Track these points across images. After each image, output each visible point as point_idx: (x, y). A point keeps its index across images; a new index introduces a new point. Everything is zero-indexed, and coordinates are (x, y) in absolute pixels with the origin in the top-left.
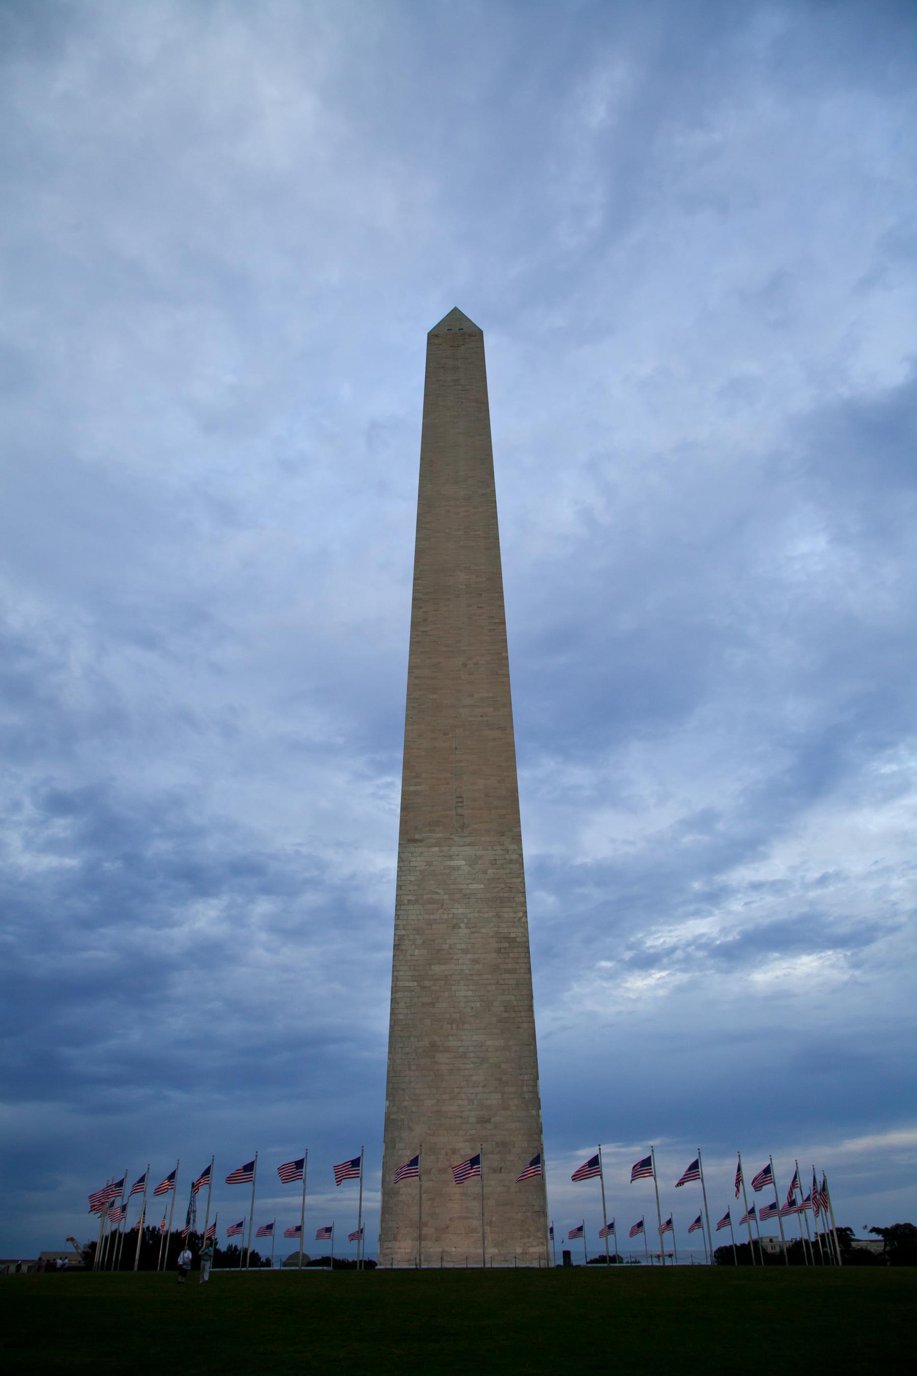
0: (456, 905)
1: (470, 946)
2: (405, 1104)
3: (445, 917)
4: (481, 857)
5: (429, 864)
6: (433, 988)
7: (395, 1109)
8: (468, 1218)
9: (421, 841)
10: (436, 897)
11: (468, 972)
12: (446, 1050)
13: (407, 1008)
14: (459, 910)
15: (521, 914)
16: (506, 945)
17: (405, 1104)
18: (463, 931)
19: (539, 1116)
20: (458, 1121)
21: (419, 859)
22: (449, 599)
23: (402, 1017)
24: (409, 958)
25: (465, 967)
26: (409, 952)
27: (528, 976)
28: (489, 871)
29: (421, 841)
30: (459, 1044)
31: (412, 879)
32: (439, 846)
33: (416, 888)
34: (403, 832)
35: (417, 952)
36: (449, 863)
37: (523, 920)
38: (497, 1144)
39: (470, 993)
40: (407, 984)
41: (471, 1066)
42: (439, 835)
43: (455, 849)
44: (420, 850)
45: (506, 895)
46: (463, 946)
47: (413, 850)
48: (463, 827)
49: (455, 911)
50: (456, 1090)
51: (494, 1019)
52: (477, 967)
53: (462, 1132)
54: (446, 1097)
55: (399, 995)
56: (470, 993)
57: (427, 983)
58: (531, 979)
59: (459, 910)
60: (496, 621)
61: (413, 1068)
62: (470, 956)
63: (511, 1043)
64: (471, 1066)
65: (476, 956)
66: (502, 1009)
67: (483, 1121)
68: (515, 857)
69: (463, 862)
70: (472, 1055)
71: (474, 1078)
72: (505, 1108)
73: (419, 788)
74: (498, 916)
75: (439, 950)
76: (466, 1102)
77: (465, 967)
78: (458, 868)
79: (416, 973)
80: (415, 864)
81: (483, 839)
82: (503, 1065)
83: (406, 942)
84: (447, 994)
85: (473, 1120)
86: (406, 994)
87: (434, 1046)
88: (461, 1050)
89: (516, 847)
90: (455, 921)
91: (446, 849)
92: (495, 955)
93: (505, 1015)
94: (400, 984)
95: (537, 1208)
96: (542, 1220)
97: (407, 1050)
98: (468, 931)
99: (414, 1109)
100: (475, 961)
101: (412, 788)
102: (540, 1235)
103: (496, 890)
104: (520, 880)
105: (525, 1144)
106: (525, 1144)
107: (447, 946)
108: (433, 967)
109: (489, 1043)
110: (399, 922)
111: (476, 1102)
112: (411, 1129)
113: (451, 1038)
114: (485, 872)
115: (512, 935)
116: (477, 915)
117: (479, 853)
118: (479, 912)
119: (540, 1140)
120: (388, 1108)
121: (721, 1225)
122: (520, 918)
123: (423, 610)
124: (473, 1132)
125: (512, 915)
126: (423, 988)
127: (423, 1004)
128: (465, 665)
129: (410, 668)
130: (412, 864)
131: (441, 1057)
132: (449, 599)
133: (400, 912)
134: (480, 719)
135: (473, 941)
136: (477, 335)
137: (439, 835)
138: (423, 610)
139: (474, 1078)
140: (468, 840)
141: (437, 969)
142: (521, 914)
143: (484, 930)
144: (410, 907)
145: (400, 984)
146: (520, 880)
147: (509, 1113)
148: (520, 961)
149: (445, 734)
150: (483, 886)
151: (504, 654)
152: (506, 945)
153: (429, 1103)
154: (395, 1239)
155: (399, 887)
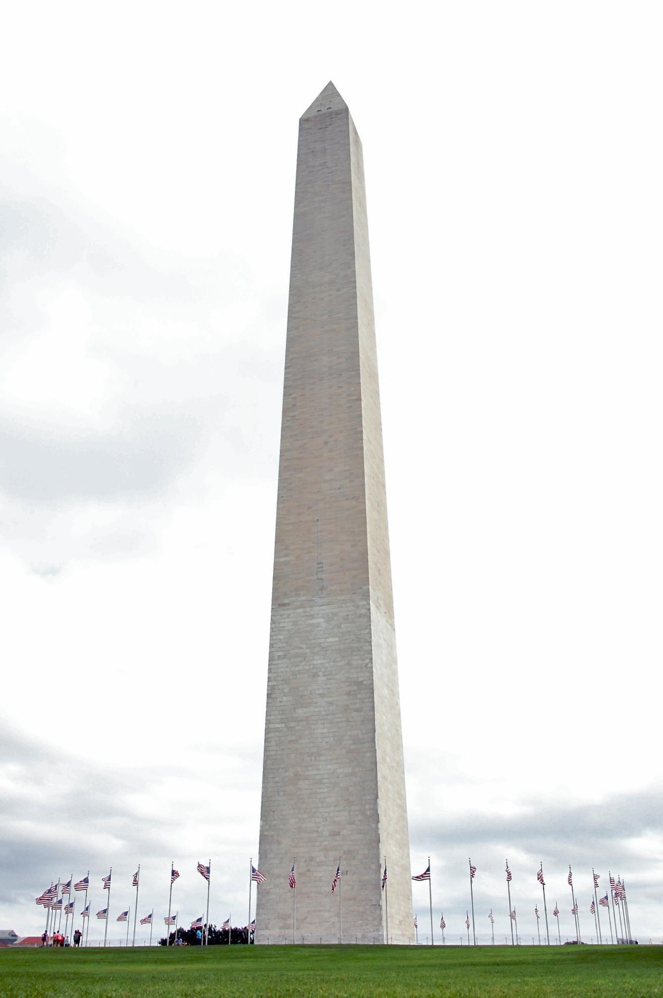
0: (316, 657)
1: (326, 691)
2: (274, 823)
3: (307, 667)
4: (336, 614)
5: (295, 623)
6: (297, 728)
7: (267, 827)
8: (320, 911)
9: (289, 604)
10: (301, 651)
11: (324, 713)
12: (307, 778)
13: (277, 745)
14: (318, 661)
16: (355, 688)
17: (274, 823)
18: (322, 679)
19: (377, 828)
20: (314, 835)
21: (287, 620)
22: (313, 384)
23: (273, 753)
24: (278, 704)
25: (322, 709)
26: (279, 700)
27: (371, 713)
28: (343, 626)
29: (289, 604)
30: (316, 772)
31: (281, 637)
32: (304, 607)
33: (285, 645)
34: (275, 599)
35: (285, 699)
36: (311, 622)
37: (369, 665)
38: (345, 852)
39: (325, 730)
40: (277, 726)
41: (326, 790)
43: (316, 609)
45: (356, 645)
46: (321, 691)
47: (282, 612)
48: (322, 589)
49: (315, 662)
50: (314, 810)
51: (344, 751)
52: (331, 708)
53: (317, 844)
54: (305, 816)
56: (325, 730)
57: (292, 724)
58: (374, 715)
59: (318, 661)
60: (354, 398)
61: (281, 794)
62: (326, 699)
63: (357, 769)
64: (326, 790)
65: (331, 699)
66: (351, 742)
67: (335, 834)
68: (363, 611)
69: (322, 620)
70: (326, 781)
71: (328, 800)
72: (352, 823)
73: (287, 559)
74: (349, 664)
75: (302, 696)
76: (321, 820)
77: (322, 709)
78: (318, 625)
79: (283, 716)
80: (284, 625)
81: (338, 598)
82: (351, 789)
83: (277, 691)
84: (307, 732)
85: (326, 833)
86: (278, 734)
87: (296, 774)
88: (318, 777)
89: (365, 603)
90: (314, 671)
91: (308, 609)
92: (345, 697)
93: (353, 747)
94: (271, 726)
95: (374, 903)
96: (378, 912)
97: (277, 780)
98: (325, 678)
99: (281, 827)
100: (331, 703)
101: (283, 559)
102: (376, 923)
103: (348, 641)
104: (367, 631)
105: (366, 852)
106: (366, 852)
107: (308, 692)
108: (297, 711)
109: (339, 771)
110: (271, 675)
111: (329, 819)
112: (279, 843)
113: (310, 768)
114: (339, 627)
116: (332, 664)
117: (335, 611)
118: (334, 661)
119: (378, 848)
120: (261, 827)
121: (144, 921)
122: (367, 664)
124: (326, 843)
125: (360, 662)
126: (289, 728)
127: (290, 742)
129: (281, 451)
130: (281, 625)
131: (302, 784)
132: (313, 384)
133: (272, 667)
134: (338, 491)
135: (329, 686)
136: (343, 113)
137: (304, 598)
138: (294, 396)
139: (328, 800)
140: (326, 600)
141: (301, 712)
142: (367, 661)
143: (338, 677)
144: (279, 662)
145: (271, 726)
146: (367, 631)
147: (354, 827)
148: (366, 700)
149: (309, 508)
150: (337, 639)
151: (359, 429)
153: (293, 821)
154: (267, 928)
155: (271, 646)
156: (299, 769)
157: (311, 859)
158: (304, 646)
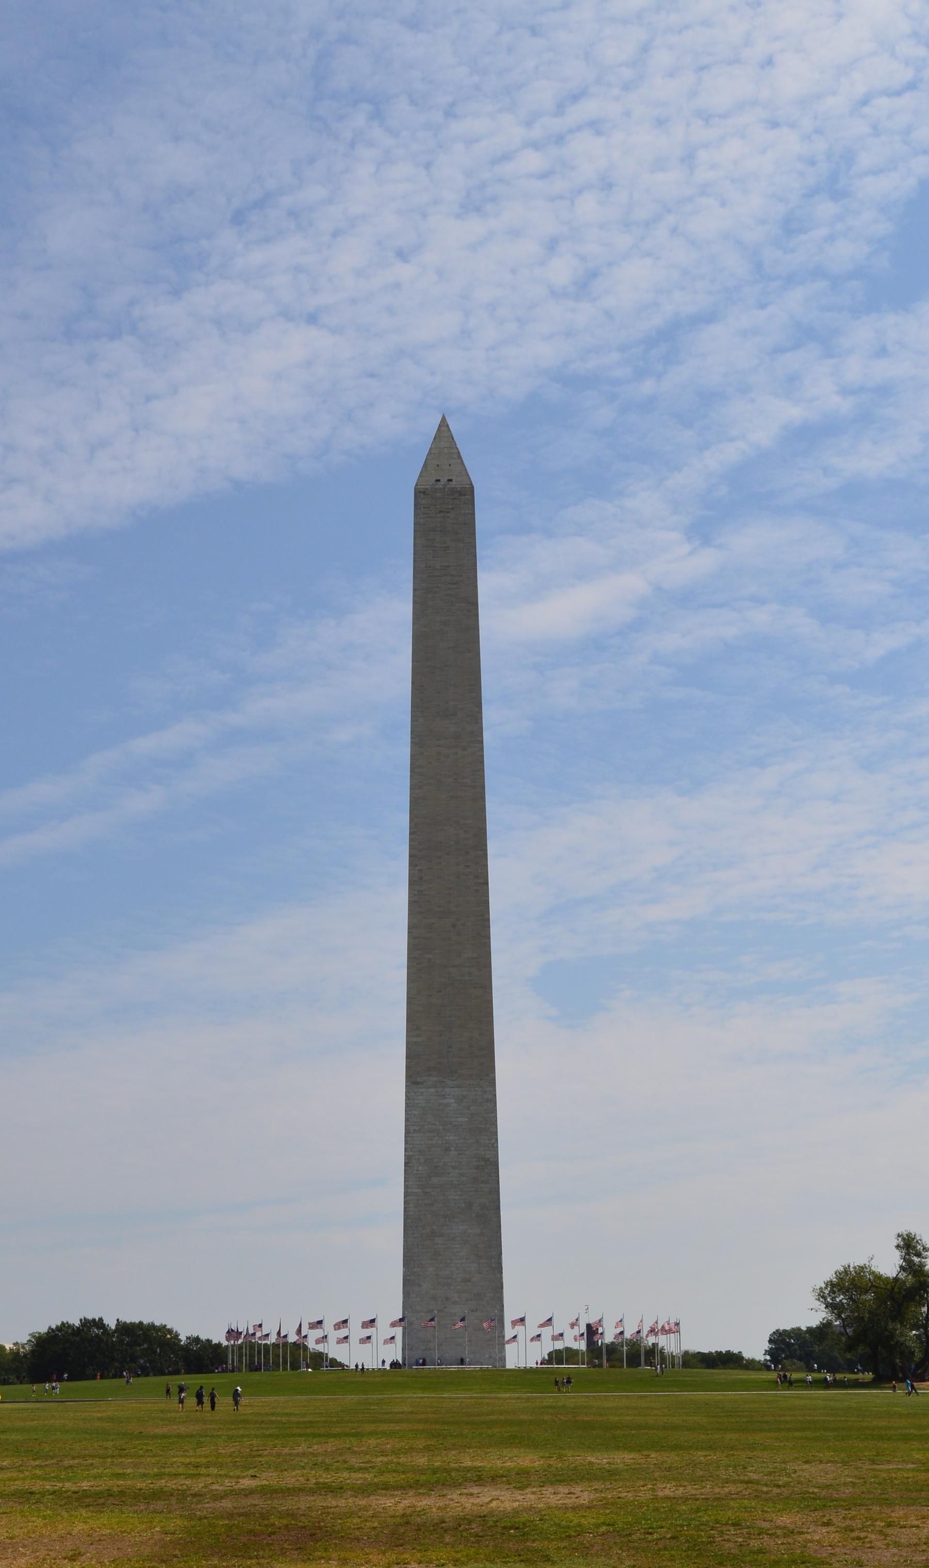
9: (422, 1083)
15: (493, 1141)
16: (483, 1163)
21: (420, 1097)
23: (411, 1213)
29: (422, 1083)
31: (416, 1113)
35: (420, 1168)
42: (435, 1079)
43: (447, 1090)
44: (421, 1090)
46: (453, 1164)
55: (410, 1198)
56: (457, 1197)
57: (428, 1190)
68: (490, 1097)
98: (456, 1153)
101: (415, 1039)
112: (419, 1285)
115: (488, 1156)
116: (462, 1141)
123: (418, 868)
128: (454, 926)
132: (440, 857)
141: (435, 1180)
152: (483, 1163)
153: (431, 1269)
156: (435, 1228)
157: (447, 1299)
158: (437, 1123)
